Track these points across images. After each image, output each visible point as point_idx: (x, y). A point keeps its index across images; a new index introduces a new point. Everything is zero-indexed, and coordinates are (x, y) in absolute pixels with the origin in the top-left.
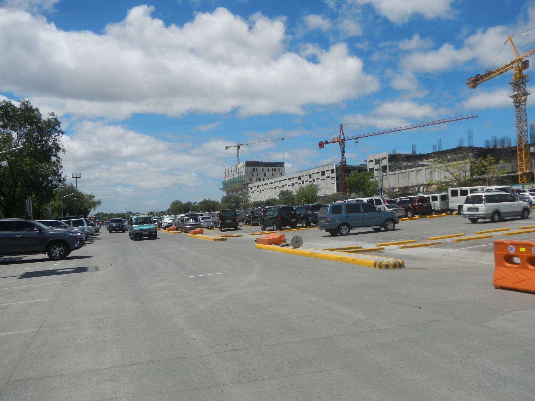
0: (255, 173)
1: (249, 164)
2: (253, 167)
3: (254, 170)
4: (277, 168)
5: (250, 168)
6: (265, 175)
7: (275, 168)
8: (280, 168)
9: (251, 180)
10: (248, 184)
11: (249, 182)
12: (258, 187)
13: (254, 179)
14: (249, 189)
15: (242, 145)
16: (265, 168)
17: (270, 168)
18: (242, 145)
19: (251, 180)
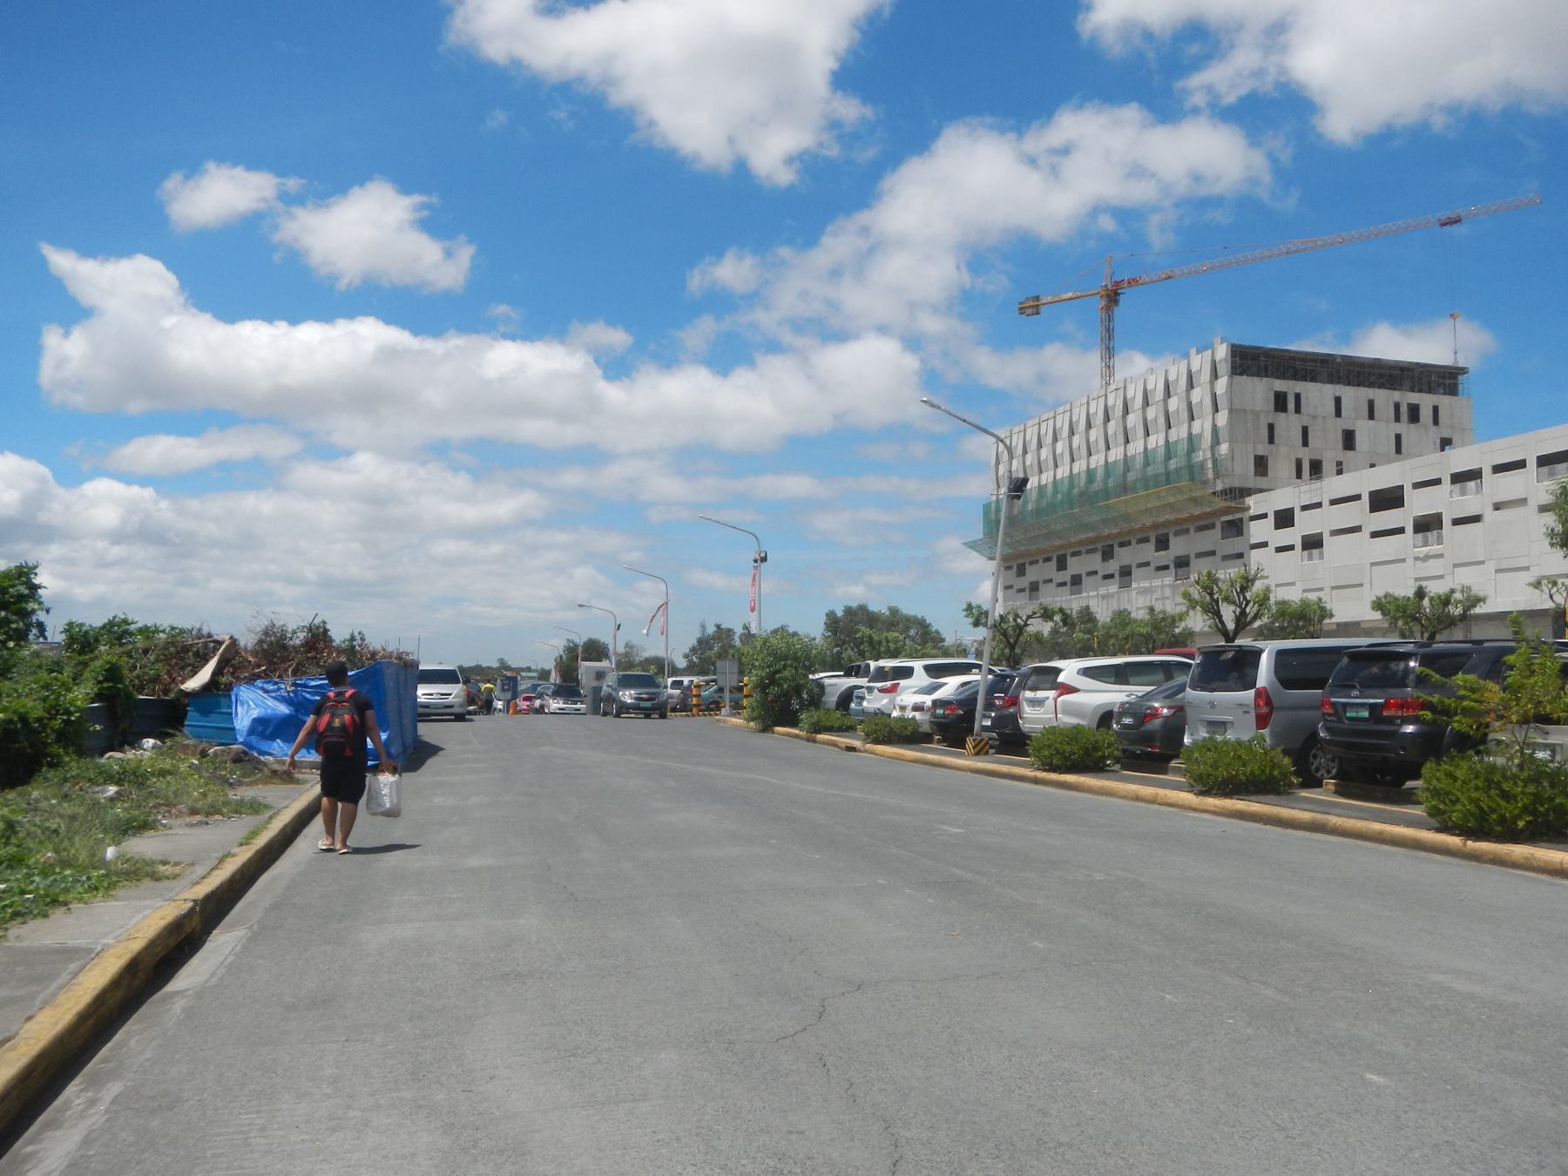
0: (1288, 425)
1: (1247, 361)
2: (1280, 385)
3: (1280, 402)
4: (1425, 401)
5: (1259, 390)
6: (1349, 440)
7: (1414, 398)
8: (1444, 401)
9: (1261, 465)
10: (1246, 492)
11: (1252, 481)
12: (1387, 499)
13: (1281, 466)
14: (1259, 531)
15: (1133, 282)
16: (1353, 396)
17: (1384, 398)
18: (1133, 282)
19: (1261, 465)
